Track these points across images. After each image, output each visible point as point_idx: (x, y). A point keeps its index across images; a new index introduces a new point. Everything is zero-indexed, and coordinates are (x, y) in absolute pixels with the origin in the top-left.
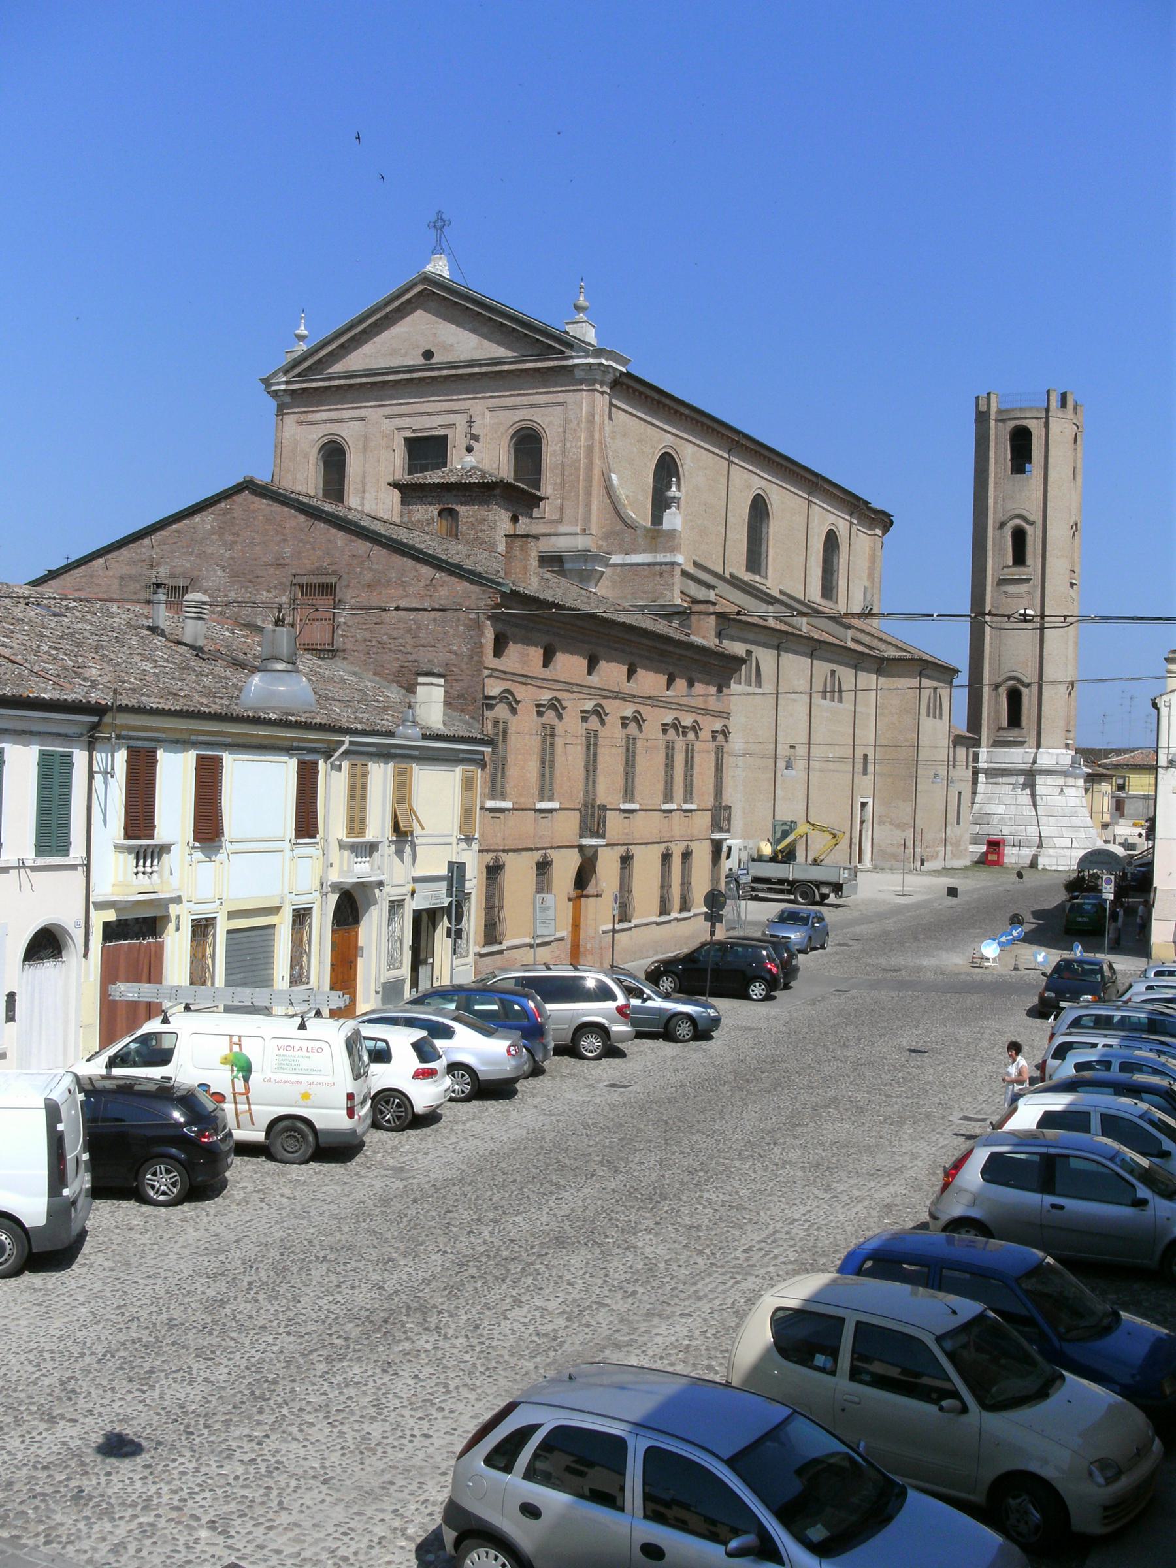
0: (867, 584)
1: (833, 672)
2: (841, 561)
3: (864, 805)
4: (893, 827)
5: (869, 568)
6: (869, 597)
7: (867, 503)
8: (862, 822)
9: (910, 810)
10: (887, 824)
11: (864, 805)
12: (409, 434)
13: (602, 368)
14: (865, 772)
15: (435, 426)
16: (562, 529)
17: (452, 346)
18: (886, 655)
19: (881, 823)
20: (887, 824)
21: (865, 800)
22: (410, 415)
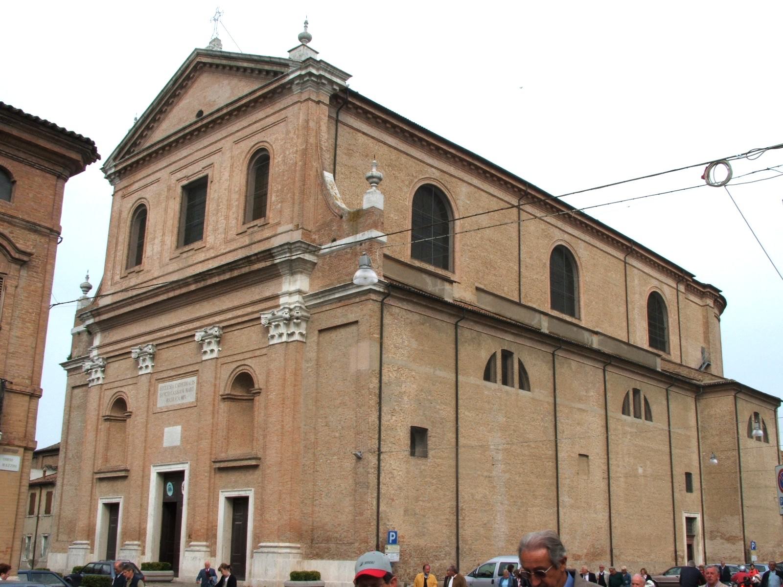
0: (704, 345)
1: (636, 392)
2: (670, 320)
3: (690, 521)
4: (724, 541)
5: (704, 333)
6: (706, 355)
7: (692, 276)
8: (691, 536)
9: (737, 523)
10: (718, 538)
11: (690, 521)
12: (185, 182)
13: (315, 79)
14: (689, 489)
15: (201, 169)
16: (280, 229)
17: (215, 101)
18: (702, 383)
19: (712, 538)
20: (718, 538)
21: (692, 516)
22: (186, 166)
